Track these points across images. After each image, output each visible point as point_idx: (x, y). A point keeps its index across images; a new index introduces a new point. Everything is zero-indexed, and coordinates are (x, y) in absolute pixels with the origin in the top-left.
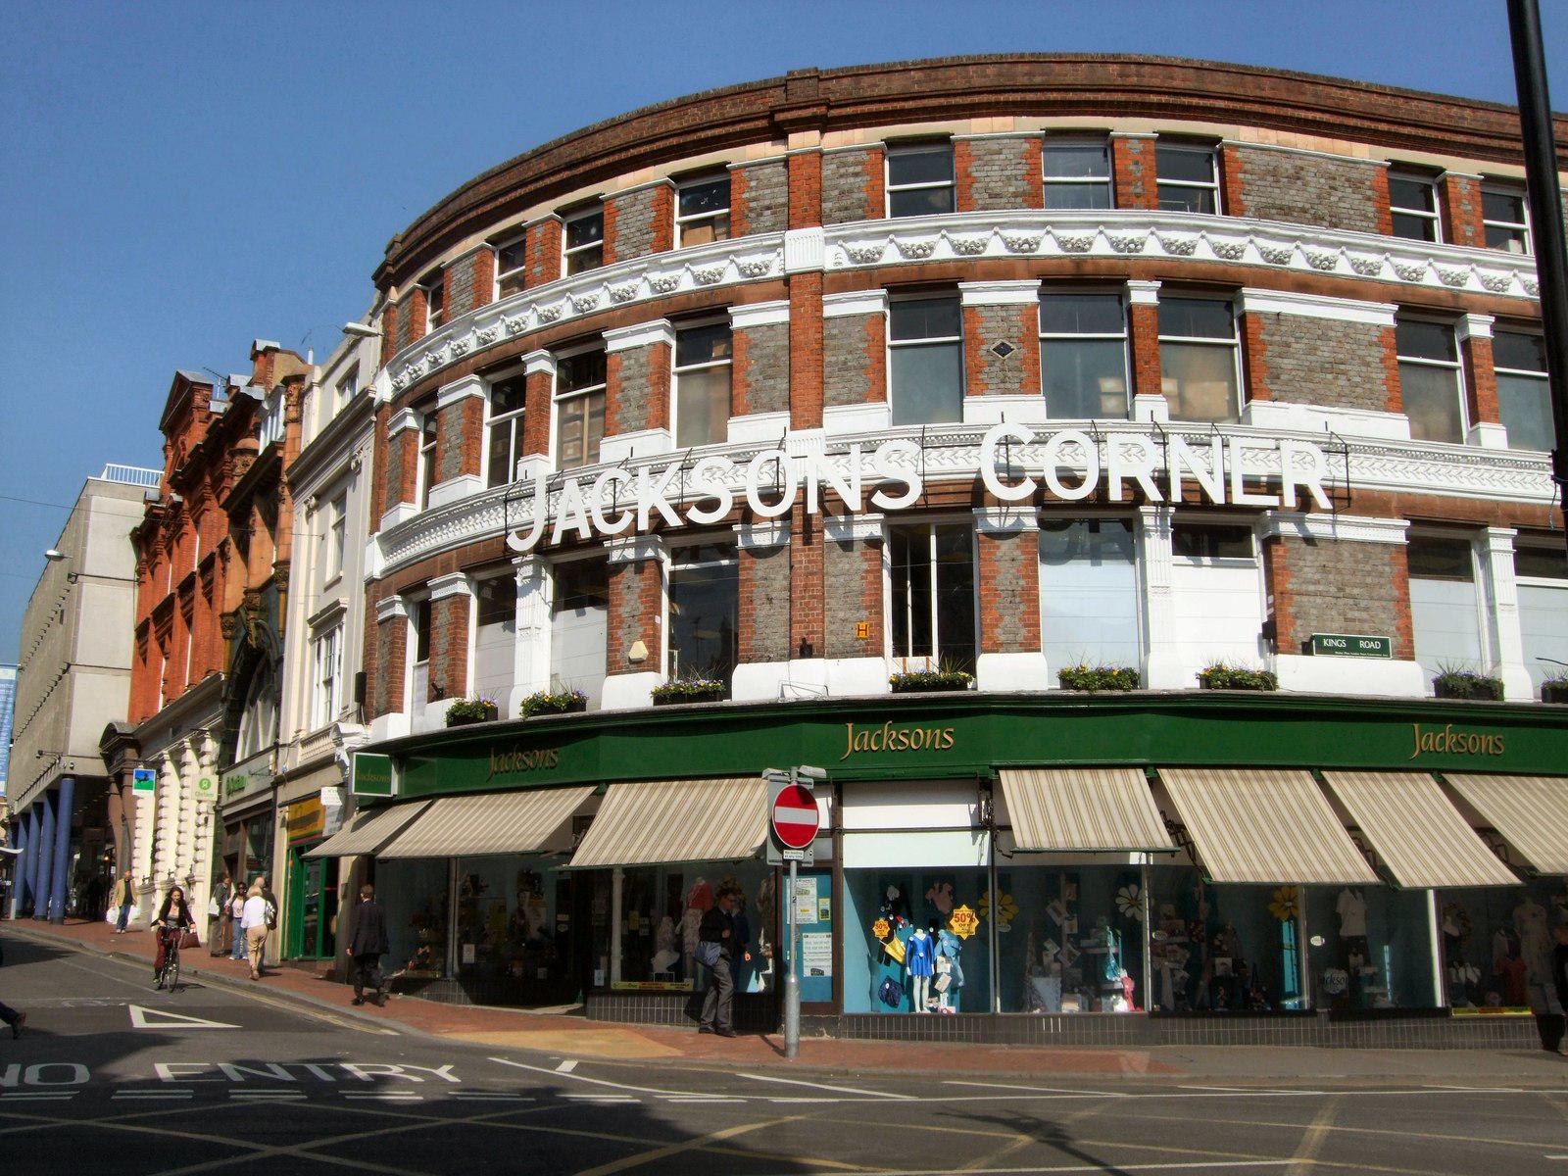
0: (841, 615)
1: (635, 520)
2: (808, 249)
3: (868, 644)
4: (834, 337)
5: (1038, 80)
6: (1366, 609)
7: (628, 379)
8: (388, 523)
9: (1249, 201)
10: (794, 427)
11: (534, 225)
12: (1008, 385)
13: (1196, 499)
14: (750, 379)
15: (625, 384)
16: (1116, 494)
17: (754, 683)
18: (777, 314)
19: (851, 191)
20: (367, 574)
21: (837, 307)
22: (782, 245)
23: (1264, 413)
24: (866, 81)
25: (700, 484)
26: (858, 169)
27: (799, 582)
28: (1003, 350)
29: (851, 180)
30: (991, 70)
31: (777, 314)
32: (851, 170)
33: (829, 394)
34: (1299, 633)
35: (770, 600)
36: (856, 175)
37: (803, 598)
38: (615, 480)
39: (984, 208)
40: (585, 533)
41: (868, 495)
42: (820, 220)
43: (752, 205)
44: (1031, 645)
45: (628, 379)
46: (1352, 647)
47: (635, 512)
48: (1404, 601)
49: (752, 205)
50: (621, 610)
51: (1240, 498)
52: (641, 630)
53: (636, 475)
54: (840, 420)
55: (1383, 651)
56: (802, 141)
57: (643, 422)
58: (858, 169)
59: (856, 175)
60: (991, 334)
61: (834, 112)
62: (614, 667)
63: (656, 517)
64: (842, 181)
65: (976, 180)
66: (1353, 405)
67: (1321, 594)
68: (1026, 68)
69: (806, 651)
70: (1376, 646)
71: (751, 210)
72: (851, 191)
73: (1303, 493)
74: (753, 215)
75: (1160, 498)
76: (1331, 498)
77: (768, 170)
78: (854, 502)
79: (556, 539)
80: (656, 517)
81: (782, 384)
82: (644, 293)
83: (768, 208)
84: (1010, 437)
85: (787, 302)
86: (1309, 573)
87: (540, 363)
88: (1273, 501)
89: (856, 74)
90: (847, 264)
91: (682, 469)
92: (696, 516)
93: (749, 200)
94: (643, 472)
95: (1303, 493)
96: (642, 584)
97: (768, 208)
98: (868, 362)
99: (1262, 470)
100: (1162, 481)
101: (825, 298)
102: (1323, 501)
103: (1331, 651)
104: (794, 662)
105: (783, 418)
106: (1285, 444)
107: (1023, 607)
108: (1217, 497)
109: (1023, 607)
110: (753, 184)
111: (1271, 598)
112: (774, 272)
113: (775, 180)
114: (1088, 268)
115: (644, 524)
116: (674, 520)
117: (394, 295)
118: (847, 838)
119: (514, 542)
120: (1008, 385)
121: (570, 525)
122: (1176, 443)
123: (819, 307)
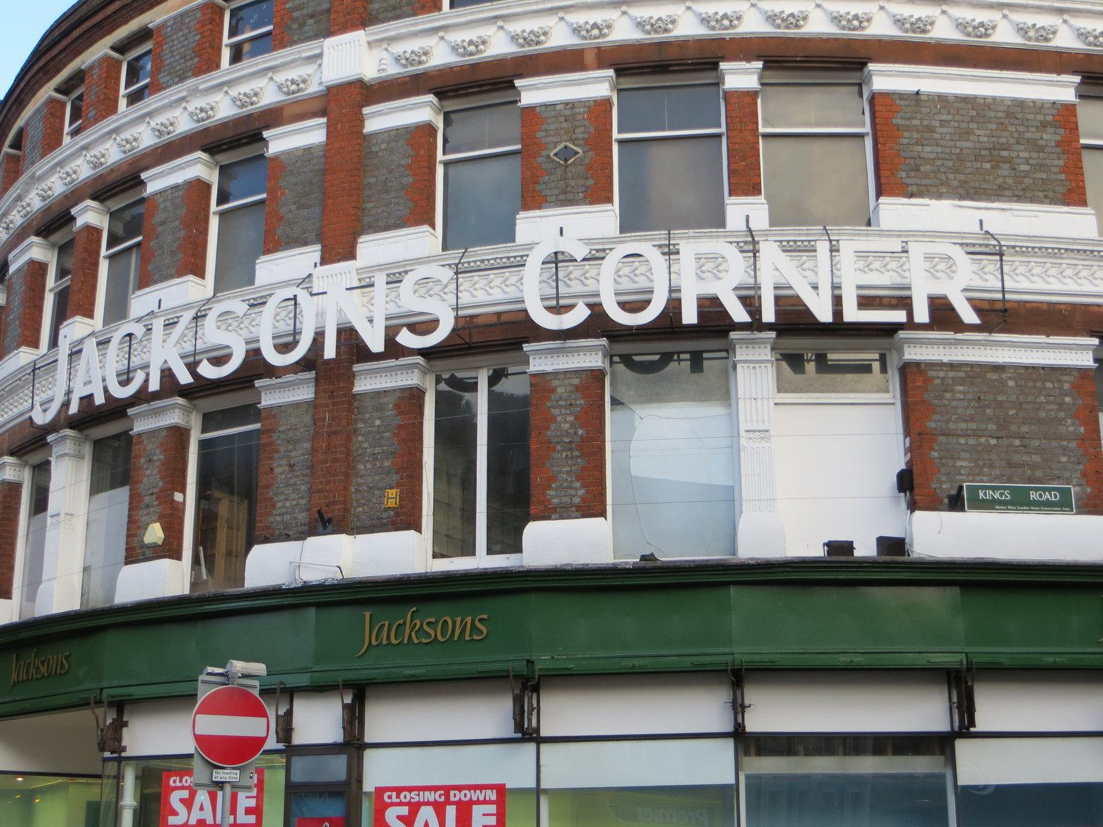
1: (146, 381)
3: (397, 514)
6: (1038, 451)
10: (324, 261)
11: (91, 67)
12: (570, 196)
16: (690, 316)
17: (268, 565)
22: (320, 56)
23: (895, 212)
25: (213, 334)
31: (308, 135)
33: (366, 220)
37: (324, 462)
38: (130, 335)
43: (295, 15)
44: (593, 507)
49: (295, 15)
51: (852, 314)
54: (375, 249)
57: (173, 271)
62: (136, 553)
66: (1019, 198)
67: (975, 434)
70: (1053, 497)
71: (294, 20)
74: (295, 26)
75: (747, 319)
76: (979, 311)
78: (376, 344)
80: (167, 375)
85: (324, 120)
88: (899, 316)
90: (393, 70)
91: (196, 318)
92: (208, 371)
93: (292, 10)
97: (312, 16)
99: (881, 279)
100: (751, 302)
101: (366, 110)
102: (969, 316)
104: (312, 541)
108: (824, 314)
112: (313, 88)
116: (184, 378)
118: (369, 755)
120: (570, 196)
122: (769, 251)
123: (361, 121)
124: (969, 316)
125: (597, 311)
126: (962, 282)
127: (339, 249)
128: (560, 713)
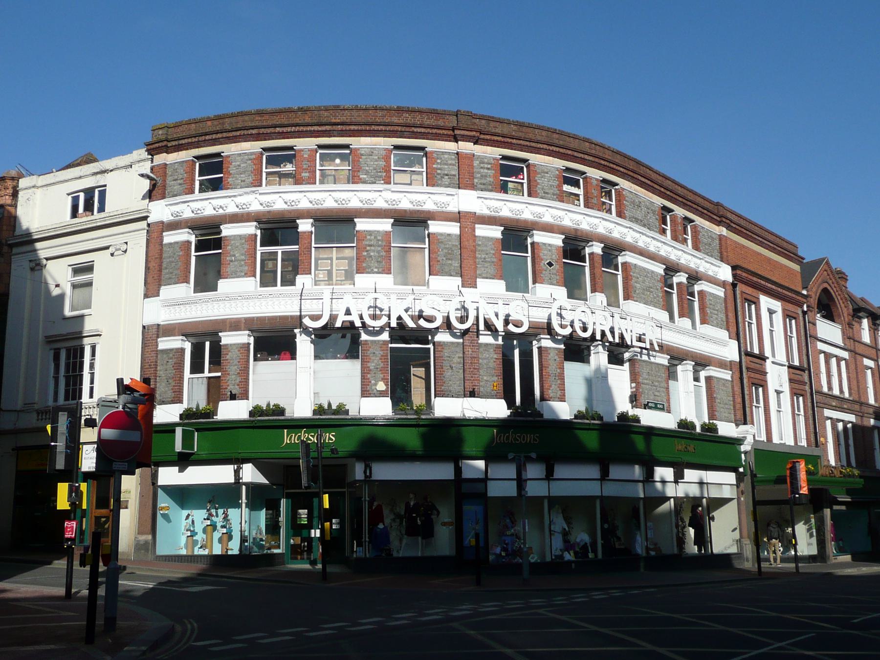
0: (485, 378)
2: (469, 201)
4: (479, 245)
5: (561, 143)
7: (370, 246)
8: (168, 292)
9: (627, 213)
13: (623, 344)
14: (439, 258)
15: (368, 248)
16: (598, 337)
18: (453, 229)
19: (486, 176)
20: (149, 320)
21: (482, 231)
24: (492, 124)
26: (489, 166)
27: (468, 361)
28: (550, 264)
29: (486, 171)
30: (544, 133)
32: (486, 166)
34: (643, 400)
35: (452, 368)
36: (488, 169)
39: (542, 198)
40: (358, 324)
41: (507, 322)
42: (473, 187)
43: (439, 171)
45: (370, 246)
46: (656, 408)
47: (389, 316)
48: (668, 388)
49: (439, 171)
50: (369, 365)
51: (635, 343)
52: (382, 376)
53: (375, 297)
55: (662, 409)
56: (466, 147)
57: (380, 270)
58: (489, 166)
59: (488, 169)
60: (546, 257)
61: (482, 136)
63: (400, 318)
64: (482, 170)
65: (538, 184)
68: (557, 136)
69: (472, 394)
70: (661, 407)
72: (486, 176)
73: (651, 344)
74: (439, 177)
77: (446, 156)
79: (338, 324)
81: (457, 264)
82: (380, 203)
83: (447, 175)
84: (544, 302)
86: (645, 375)
87: (305, 226)
89: (490, 119)
90: (486, 212)
92: (422, 322)
94: (393, 297)
95: (651, 344)
96: (382, 353)
97: (447, 175)
98: (495, 260)
101: (477, 226)
102: (657, 348)
103: (650, 408)
105: (458, 281)
106: (641, 321)
107: (559, 382)
108: (629, 343)
109: (559, 382)
110: (439, 161)
111: (634, 385)
113: (450, 162)
114: (579, 234)
115: (394, 324)
116: (411, 324)
117: (161, 159)
119: (307, 321)
121: (348, 318)
122: (617, 316)
124: (657, 348)
125: (574, 331)
126: (653, 335)
127: (469, 282)
128: (561, 471)
